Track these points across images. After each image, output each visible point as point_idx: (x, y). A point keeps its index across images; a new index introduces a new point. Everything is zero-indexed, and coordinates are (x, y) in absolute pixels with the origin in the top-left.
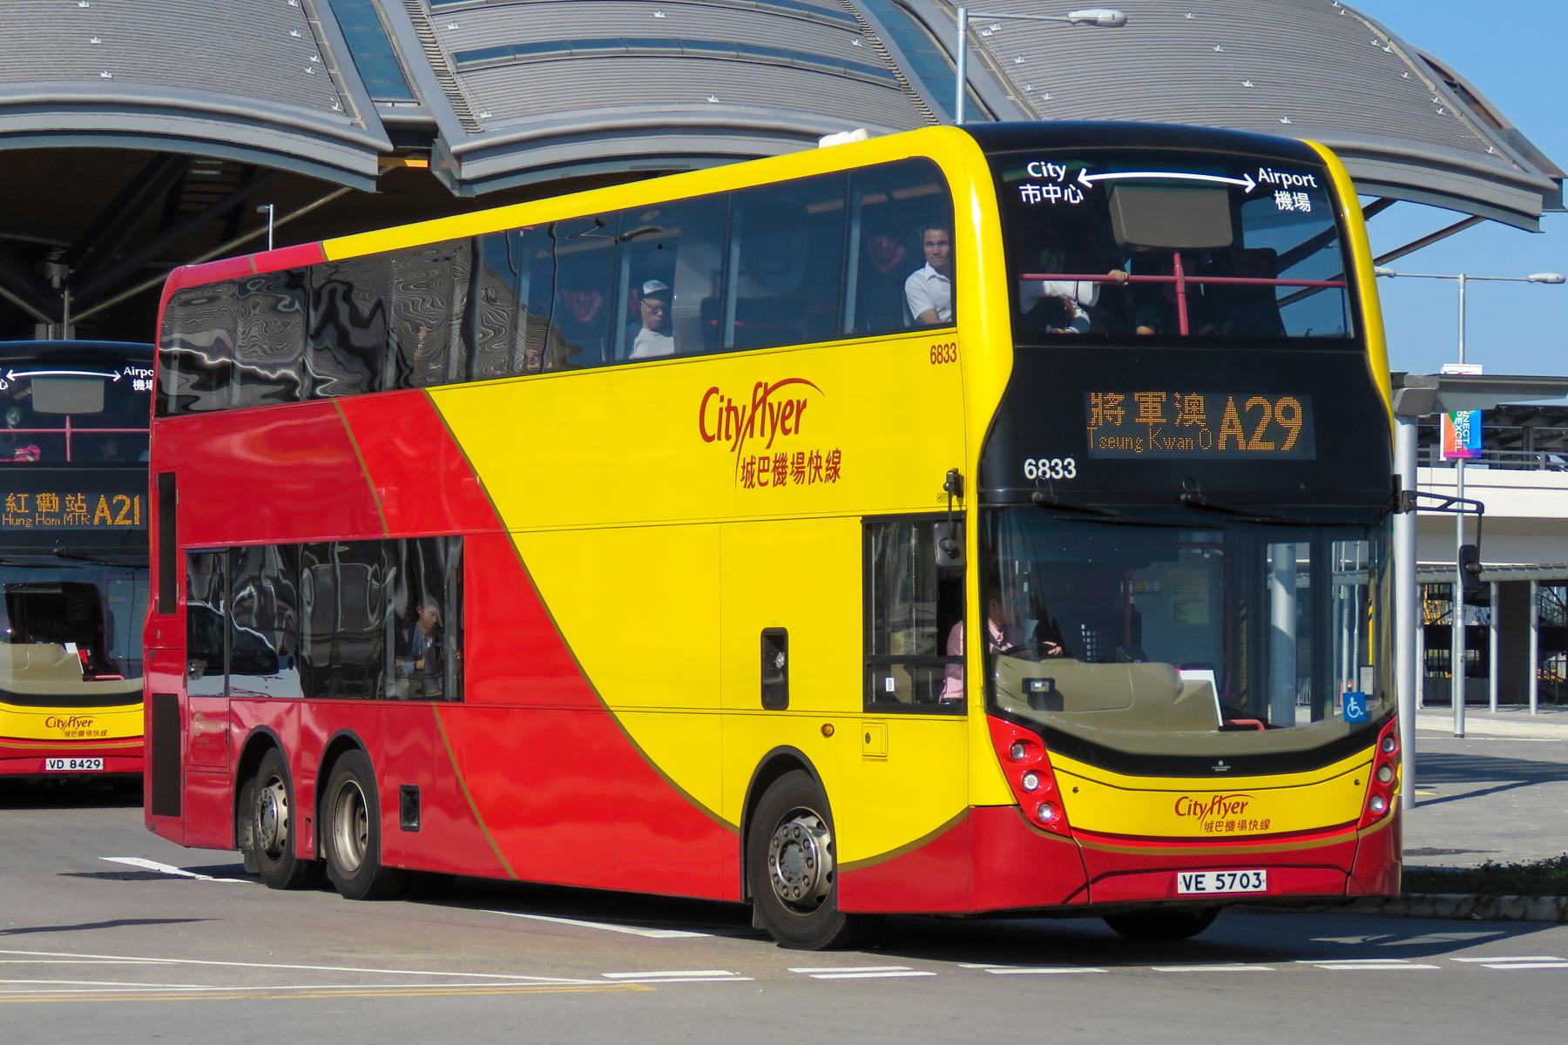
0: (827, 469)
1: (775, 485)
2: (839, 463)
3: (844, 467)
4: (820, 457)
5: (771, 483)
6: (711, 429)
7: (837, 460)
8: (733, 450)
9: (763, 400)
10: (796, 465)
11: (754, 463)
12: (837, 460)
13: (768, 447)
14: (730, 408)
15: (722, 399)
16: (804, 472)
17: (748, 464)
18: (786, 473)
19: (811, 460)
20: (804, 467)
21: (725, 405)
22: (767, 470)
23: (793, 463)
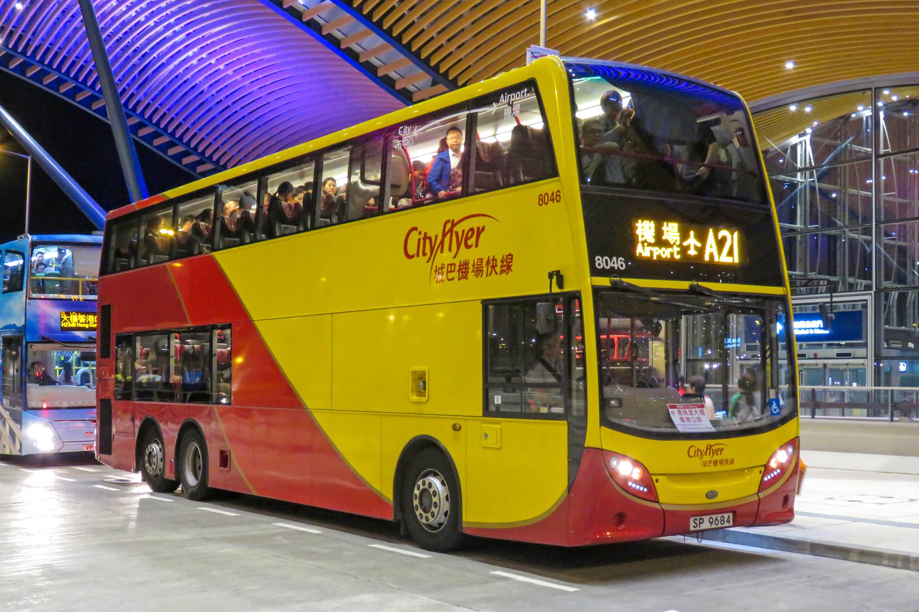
0: (501, 267)
1: (459, 279)
2: (512, 262)
3: (515, 265)
4: (496, 260)
5: (456, 278)
6: (412, 250)
7: (508, 260)
8: (428, 261)
9: (451, 230)
11: (444, 268)
12: (510, 260)
14: (425, 238)
15: (420, 233)
16: (482, 270)
17: (439, 268)
18: (468, 272)
19: (488, 262)
21: (422, 236)
22: (454, 271)
23: (474, 265)
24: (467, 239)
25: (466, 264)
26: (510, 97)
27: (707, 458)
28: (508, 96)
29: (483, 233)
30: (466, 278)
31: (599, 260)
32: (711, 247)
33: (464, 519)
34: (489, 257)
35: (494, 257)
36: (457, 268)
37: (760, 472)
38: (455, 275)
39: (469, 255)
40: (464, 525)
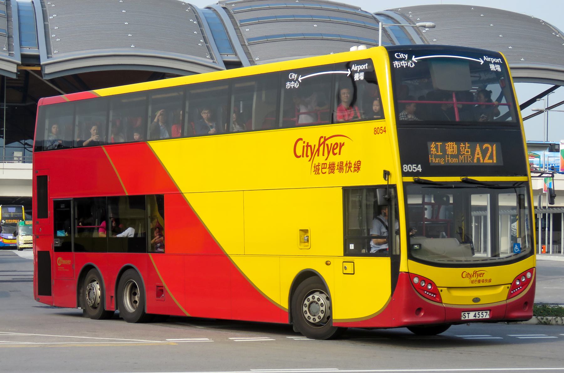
0: (354, 168)
1: (329, 173)
4: (351, 163)
5: (327, 172)
10: (339, 166)
13: (326, 160)
16: (343, 169)
18: (334, 169)
19: (346, 164)
20: (343, 167)
23: (338, 166)
24: (334, 149)
25: (334, 164)
26: (358, 67)
27: (473, 279)
28: (357, 66)
29: (343, 147)
30: (333, 172)
31: (405, 167)
32: (478, 154)
33: (334, 318)
34: (347, 161)
35: (350, 161)
36: (328, 166)
37: (508, 288)
38: (327, 170)
39: (335, 159)
40: (333, 321)
